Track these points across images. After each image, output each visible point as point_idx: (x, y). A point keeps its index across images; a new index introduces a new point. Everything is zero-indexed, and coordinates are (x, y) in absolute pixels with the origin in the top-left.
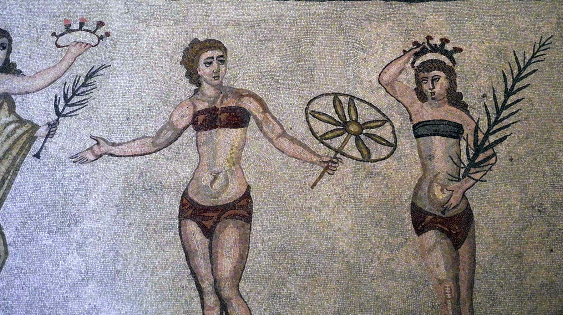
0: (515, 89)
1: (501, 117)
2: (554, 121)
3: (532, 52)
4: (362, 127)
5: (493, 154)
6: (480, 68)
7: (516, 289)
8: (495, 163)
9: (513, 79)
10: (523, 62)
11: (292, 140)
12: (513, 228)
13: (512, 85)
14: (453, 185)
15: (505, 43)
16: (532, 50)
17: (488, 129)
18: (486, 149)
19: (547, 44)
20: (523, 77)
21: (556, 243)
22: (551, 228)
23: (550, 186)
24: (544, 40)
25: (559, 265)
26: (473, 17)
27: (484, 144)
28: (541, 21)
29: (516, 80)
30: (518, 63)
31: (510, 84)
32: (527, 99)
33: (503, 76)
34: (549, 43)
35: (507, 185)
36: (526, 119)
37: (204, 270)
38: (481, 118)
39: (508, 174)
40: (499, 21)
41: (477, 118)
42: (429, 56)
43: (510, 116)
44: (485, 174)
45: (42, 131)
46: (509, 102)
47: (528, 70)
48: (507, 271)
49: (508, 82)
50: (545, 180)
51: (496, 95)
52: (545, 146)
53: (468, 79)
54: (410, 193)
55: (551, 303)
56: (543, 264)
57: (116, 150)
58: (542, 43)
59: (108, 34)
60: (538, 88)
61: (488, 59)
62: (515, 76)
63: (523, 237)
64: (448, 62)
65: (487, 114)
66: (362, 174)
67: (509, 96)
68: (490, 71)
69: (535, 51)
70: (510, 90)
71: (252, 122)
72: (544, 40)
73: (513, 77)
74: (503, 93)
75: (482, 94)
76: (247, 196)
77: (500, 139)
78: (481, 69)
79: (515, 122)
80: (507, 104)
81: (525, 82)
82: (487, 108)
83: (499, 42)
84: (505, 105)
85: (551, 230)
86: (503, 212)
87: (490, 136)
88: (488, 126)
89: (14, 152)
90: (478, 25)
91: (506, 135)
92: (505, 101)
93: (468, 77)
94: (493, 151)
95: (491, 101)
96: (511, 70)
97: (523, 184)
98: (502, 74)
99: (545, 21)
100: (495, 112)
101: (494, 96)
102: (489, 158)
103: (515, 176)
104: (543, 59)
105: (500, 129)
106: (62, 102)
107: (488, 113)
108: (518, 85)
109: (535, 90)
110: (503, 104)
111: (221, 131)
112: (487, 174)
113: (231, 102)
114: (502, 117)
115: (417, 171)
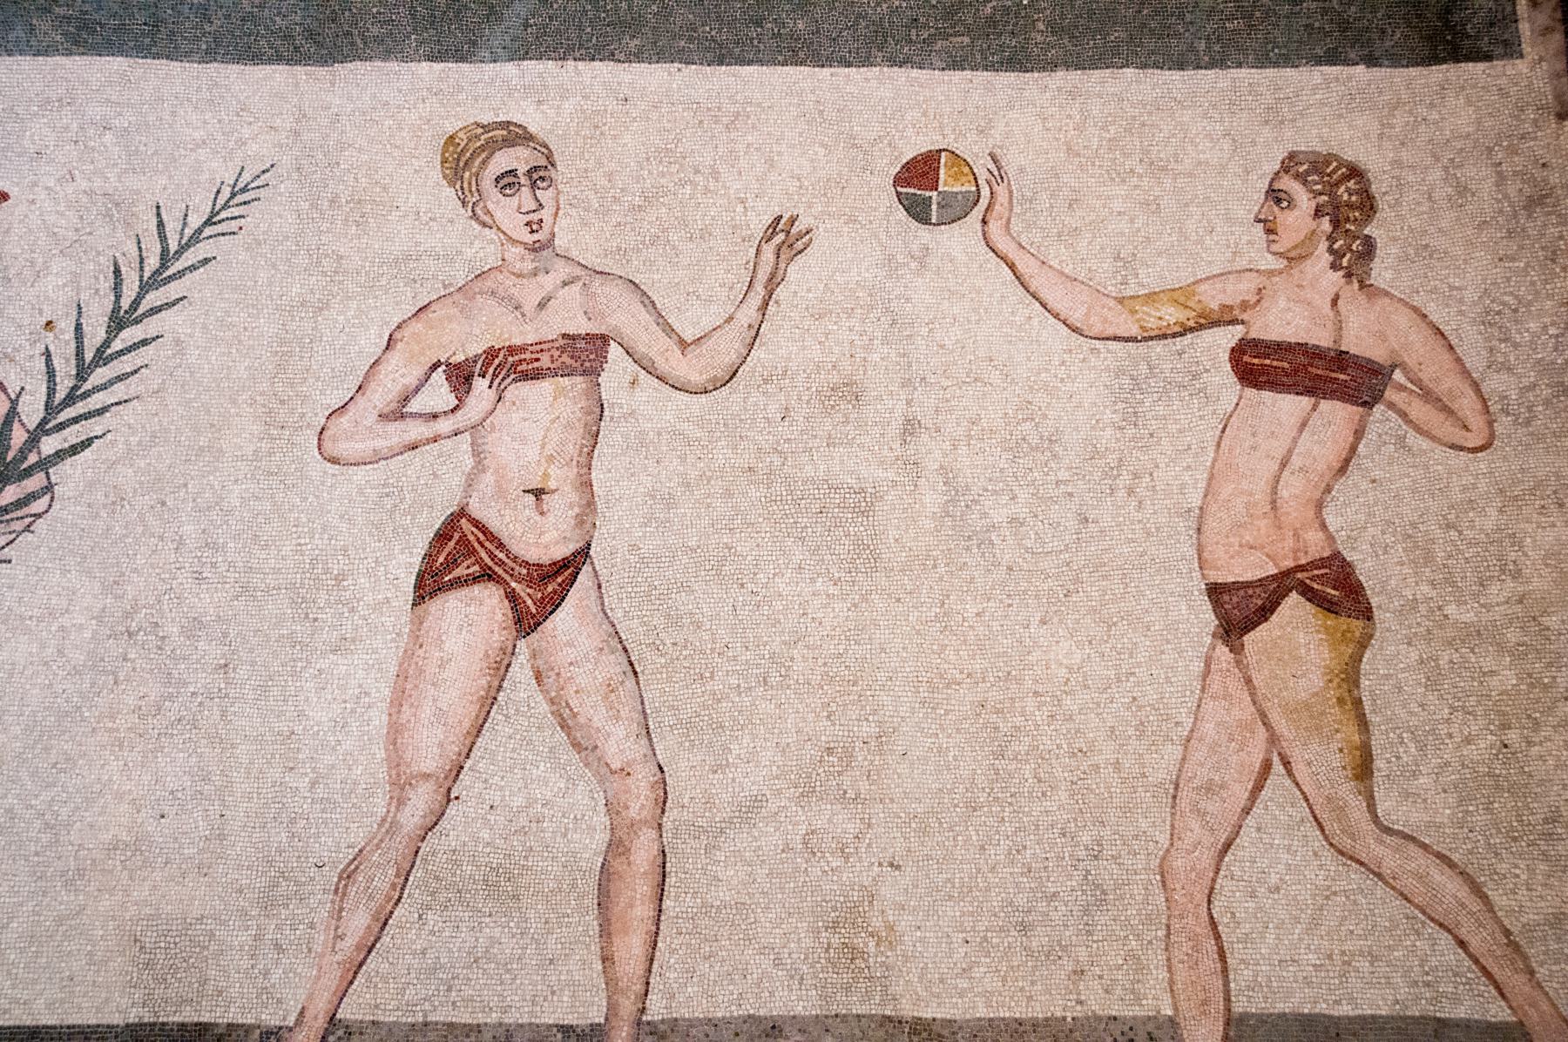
0: (140, 311)
1: (87, 386)
2: (234, 402)
3: (208, 210)
5: (46, 487)
6: (50, 250)
7: (36, 859)
8: (47, 511)
9: (141, 281)
10: (178, 237)
12: (64, 691)
13: (135, 299)
15: (133, 182)
16: (210, 204)
17: (45, 417)
18: (28, 473)
19: (253, 189)
20: (170, 277)
21: (175, 732)
22: (170, 690)
23: (189, 575)
24: (246, 177)
25: (172, 792)
26: (57, 104)
27: (26, 458)
28: (250, 123)
29: (145, 287)
30: (163, 237)
31: (130, 296)
32: (168, 338)
33: (114, 272)
34: (261, 184)
35: (69, 571)
36: (158, 392)
38: (28, 387)
39: (77, 542)
40: (130, 119)
41: (18, 389)
43: (112, 384)
44: (12, 542)
46: (117, 345)
47: (187, 258)
48: (18, 809)
49: (125, 291)
50: (180, 559)
51: (84, 325)
52: (196, 468)
53: (10, 280)
55: (128, 895)
56: (129, 787)
58: (241, 185)
60: (206, 308)
61: (80, 226)
62: (147, 275)
63: (86, 714)
65: (49, 377)
67: (120, 330)
68: (80, 259)
69: (217, 209)
70: (126, 312)
72: (246, 177)
73: (141, 277)
74: (106, 319)
75: (44, 321)
77: (73, 446)
78: (54, 252)
79: (126, 401)
80: (109, 351)
81: (172, 291)
82: (51, 360)
83: (120, 177)
84: (104, 352)
85: (170, 697)
86: (43, 646)
87: (44, 439)
88: (46, 410)
90: (66, 128)
91: (92, 435)
92: (107, 343)
93: (13, 272)
94: (45, 480)
95: (67, 342)
96: (140, 255)
97: (115, 569)
98: (112, 269)
99: (260, 124)
100: (74, 372)
101: (78, 327)
102: (32, 497)
103: (97, 549)
104: (236, 230)
105: (75, 420)
107: (51, 374)
108: (153, 299)
109: (196, 313)
110: (98, 349)
112: (16, 542)
114: (90, 387)
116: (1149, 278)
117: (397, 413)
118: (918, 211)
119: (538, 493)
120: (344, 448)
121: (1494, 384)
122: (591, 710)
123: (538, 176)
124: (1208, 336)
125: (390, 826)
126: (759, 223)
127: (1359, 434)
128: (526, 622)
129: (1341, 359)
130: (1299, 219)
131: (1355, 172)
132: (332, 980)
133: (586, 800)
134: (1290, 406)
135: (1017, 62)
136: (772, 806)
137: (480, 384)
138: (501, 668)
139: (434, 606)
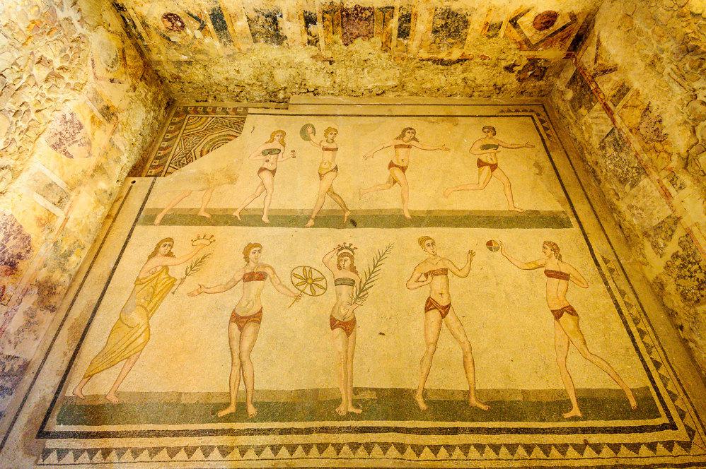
4: (313, 281)
11: (284, 286)
14: (349, 307)
37: (236, 347)
42: (344, 251)
45: (178, 282)
54: (330, 310)
57: (208, 291)
59: (214, 241)
64: (352, 254)
66: (311, 301)
71: (268, 278)
76: (261, 311)
81: (382, 262)
89: (165, 290)
106: (189, 269)
111: (254, 282)
113: (260, 270)
115: (334, 300)
116: (529, 260)
117: (417, 281)
118: (491, 249)
119: (441, 294)
120: (410, 287)
121: (585, 277)
122: (456, 332)
123: (433, 244)
124: (540, 269)
125: (427, 352)
126: (467, 251)
127: (568, 285)
128: (443, 316)
129: (561, 273)
130: (549, 251)
131: (555, 244)
132: (422, 381)
133: (458, 348)
134: (556, 281)
135: (500, 227)
136: (490, 349)
137: (429, 276)
138: (440, 324)
139: (428, 313)
